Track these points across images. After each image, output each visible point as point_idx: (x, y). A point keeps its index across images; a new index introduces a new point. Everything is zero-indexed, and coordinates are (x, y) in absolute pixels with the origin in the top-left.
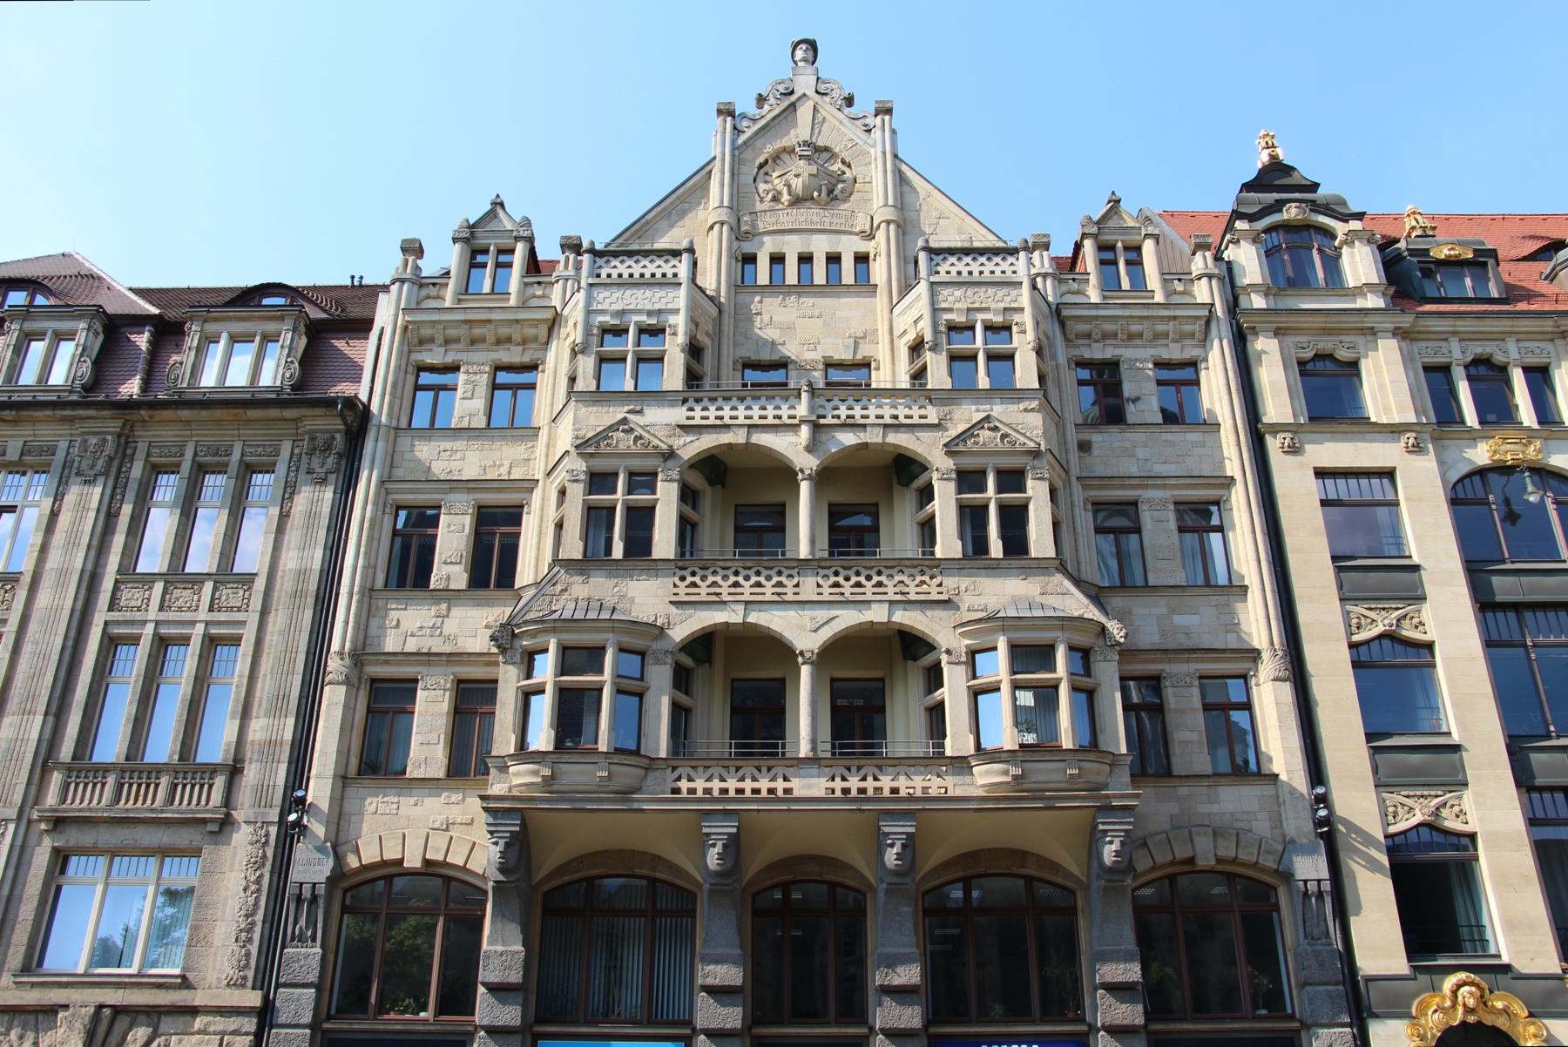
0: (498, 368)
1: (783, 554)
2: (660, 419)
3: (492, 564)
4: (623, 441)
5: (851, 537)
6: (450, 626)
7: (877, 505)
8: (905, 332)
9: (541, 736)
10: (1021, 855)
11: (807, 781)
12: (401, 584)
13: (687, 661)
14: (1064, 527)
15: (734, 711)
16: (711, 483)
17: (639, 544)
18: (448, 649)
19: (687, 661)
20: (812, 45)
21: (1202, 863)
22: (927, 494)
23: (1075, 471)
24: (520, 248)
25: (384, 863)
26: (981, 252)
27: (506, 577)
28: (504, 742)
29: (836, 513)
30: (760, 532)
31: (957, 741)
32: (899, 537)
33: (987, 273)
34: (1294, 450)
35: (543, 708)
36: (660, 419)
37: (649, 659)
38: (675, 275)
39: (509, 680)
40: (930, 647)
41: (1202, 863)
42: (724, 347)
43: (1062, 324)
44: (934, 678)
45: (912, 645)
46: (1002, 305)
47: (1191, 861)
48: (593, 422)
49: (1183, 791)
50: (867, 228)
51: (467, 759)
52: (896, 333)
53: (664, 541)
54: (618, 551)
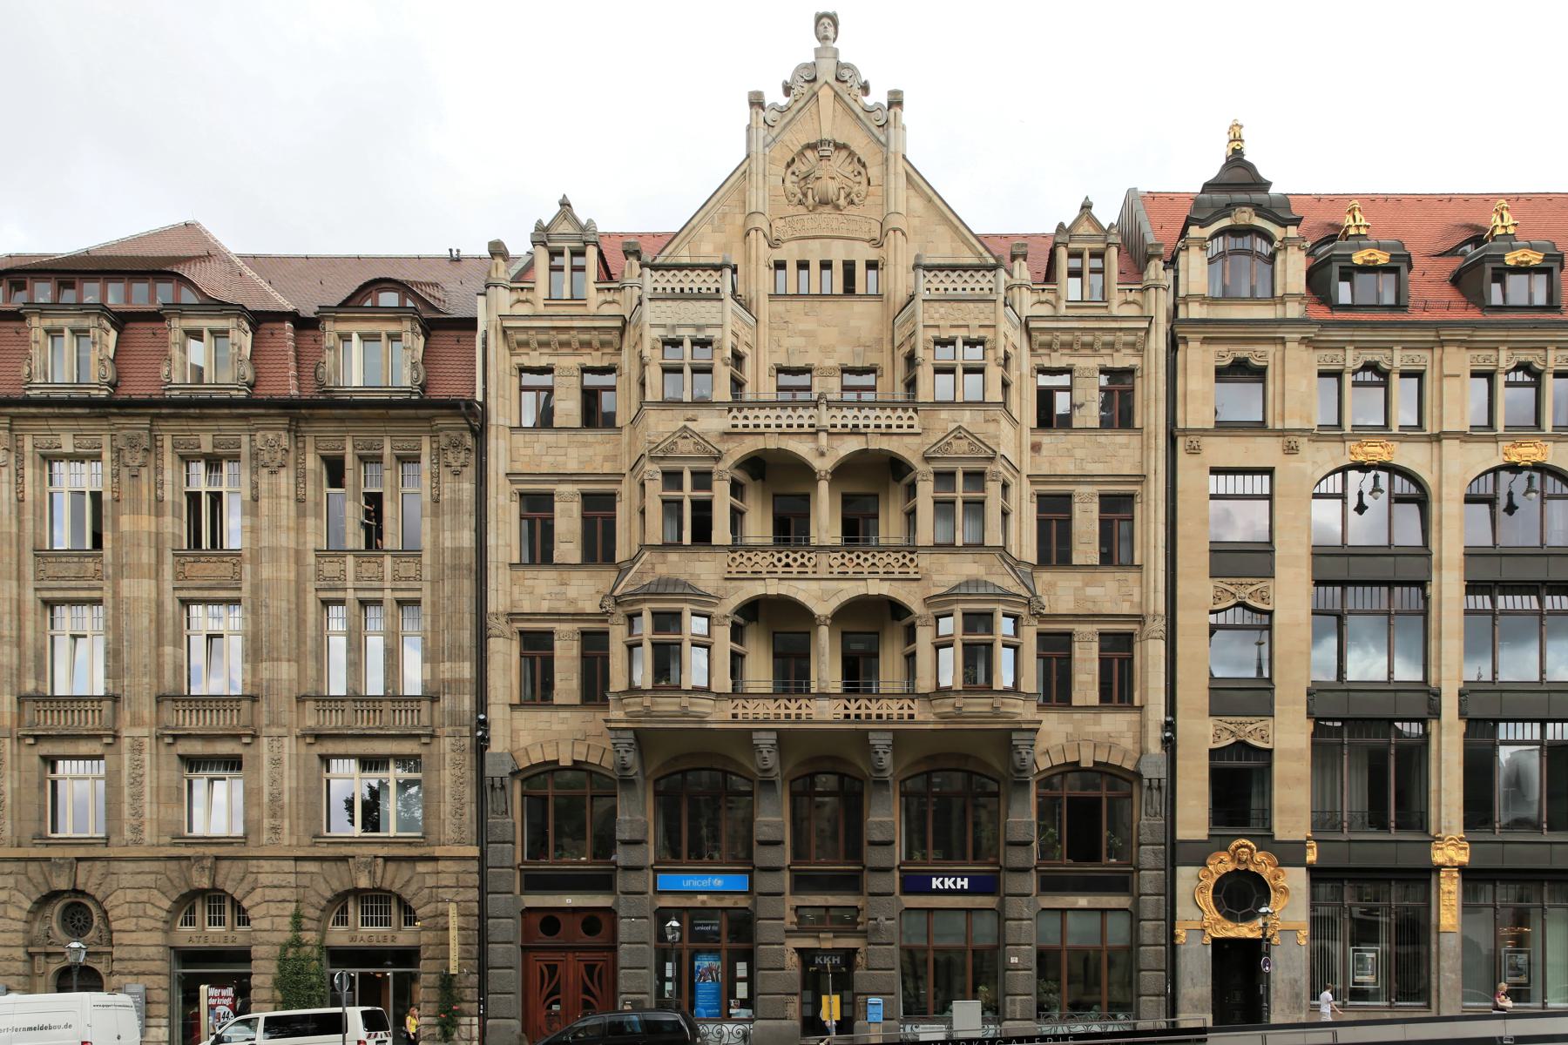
0: (586, 370)
1: (808, 540)
2: (711, 423)
3: (599, 544)
4: (686, 447)
5: (856, 529)
6: (572, 592)
7: (877, 496)
8: (902, 344)
9: (643, 675)
10: (967, 757)
11: (825, 710)
12: (532, 562)
13: (740, 620)
14: (1013, 518)
15: (775, 656)
16: (754, 479)
17: (702, 533)
18: (571, 610)
19: (740, 620)
20: (833, 19)
21: (1083, 765)
22: (911, 490)
23: (1027, 470)
24: (592, 252)
25: (546, 763)
26: (965, 268)
27: (609, 557)
28: (618, 682)
29: (847, 500)
30: (790, 527)
31: (924, 684)
32: (890, 526)
33: (968, 291)
34: (1194, 451)
35: (645, 655)
36: (711, 423)
37: (715, 621)
38: (718, 290)
39: (618, 636)
40: (909, 612)
41: (1083, 765)
42: (761, 356)
43: (1028, 332)
44: (911, 635)
45: (895, 610)
46: (977, 323)
47: (1077, 763)
48: (661, 429)
49: (1077, 716)
50: (877, 235)
51: (594, 688)
52: (897, 343)
53: (721, 532)
54: (687, 538)
